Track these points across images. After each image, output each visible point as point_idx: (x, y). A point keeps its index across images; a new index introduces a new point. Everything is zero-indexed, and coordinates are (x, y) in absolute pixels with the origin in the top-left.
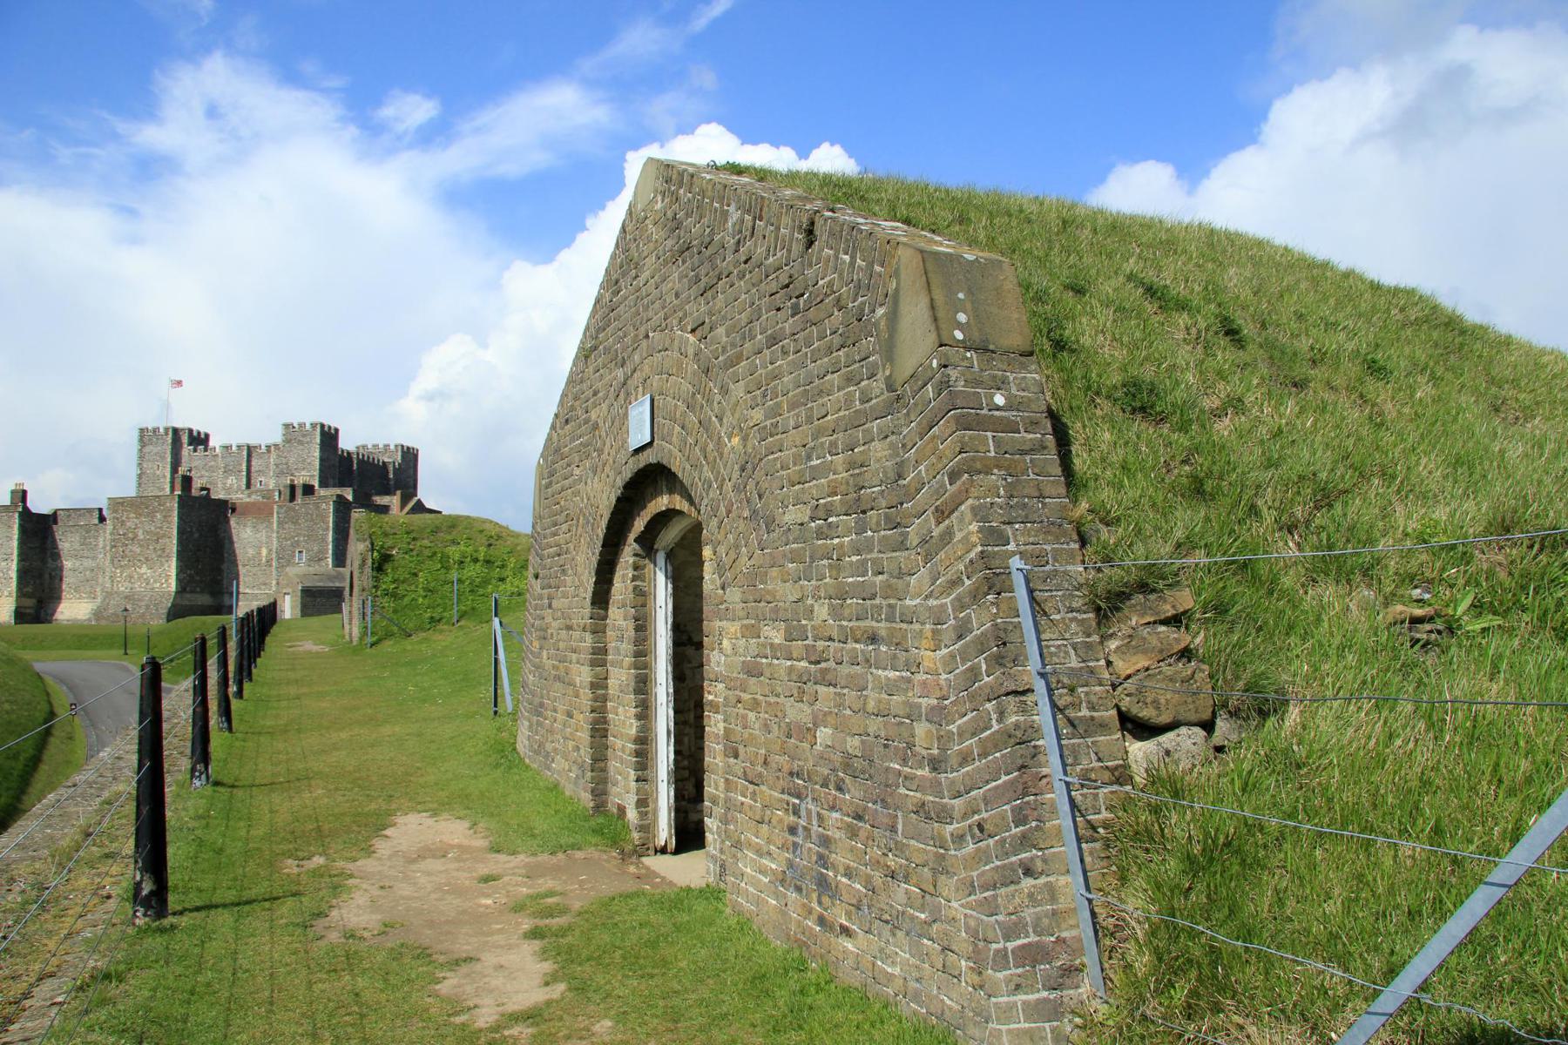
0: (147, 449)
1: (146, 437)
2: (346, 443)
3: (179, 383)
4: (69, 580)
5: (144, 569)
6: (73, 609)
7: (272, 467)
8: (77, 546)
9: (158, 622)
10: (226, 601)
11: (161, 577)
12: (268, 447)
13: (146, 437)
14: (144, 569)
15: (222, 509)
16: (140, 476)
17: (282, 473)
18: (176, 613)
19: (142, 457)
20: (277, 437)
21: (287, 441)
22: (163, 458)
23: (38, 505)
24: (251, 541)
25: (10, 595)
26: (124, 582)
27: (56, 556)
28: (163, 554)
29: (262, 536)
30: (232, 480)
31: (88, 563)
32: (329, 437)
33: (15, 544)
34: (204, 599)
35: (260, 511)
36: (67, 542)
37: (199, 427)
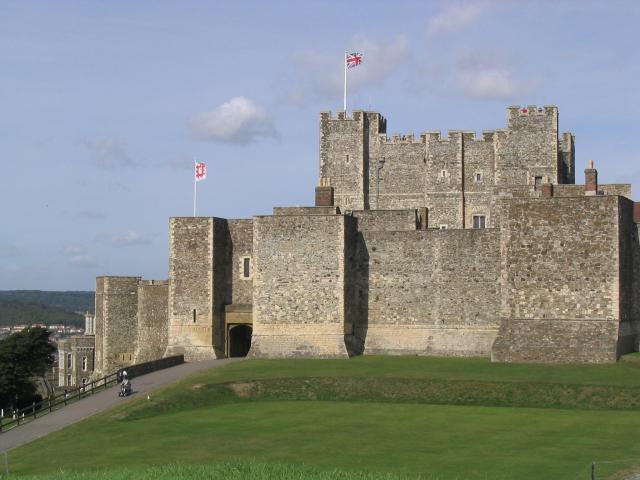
0: (332, 137)
3: (358, 60)
5: (565, 291)
7: (497, 158)
8: (400, 257)
12: (489, 137)
14: (565, 291)
16: (324, 169)
17: (509, 165)
19: (326, 146)
20: (501, 122)
21: (516, 128)
22: (353, 147)
25: (336, 319)
31: (421, 280)
33: (341, 255)
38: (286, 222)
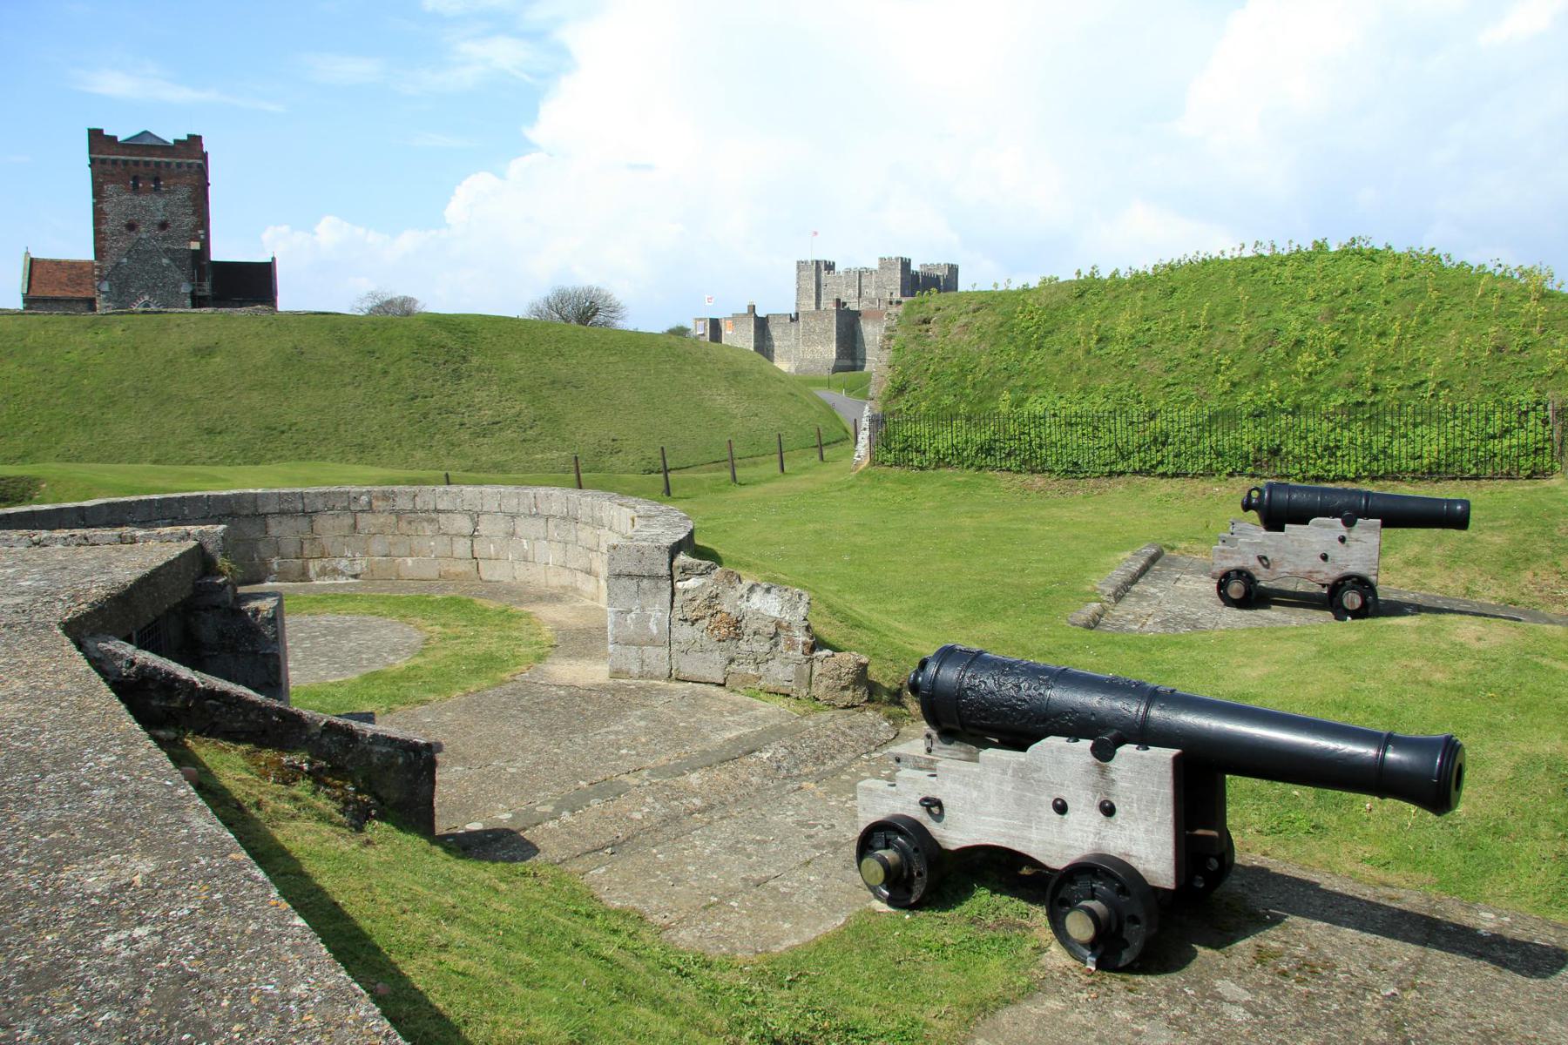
1: (801, 266)
2: (915, 267)
4: (777, 351)
6: (783, 365)
9: (826, 374)
10: (859, 363)
11: (830, 352)
13: (801, 266)
15: (857, 314)
18: (836, 369)
20: (875, 266)
23: (761, 313)
24: (871, 333)
26: (805, 353)
27: (770, 339)
28: (829, 340)
29: (877, 330)
30: (850, 291)
32: (906, 264)
34: (848, 363)
35: (876, 316)
36: (775, 332)
37: (829, 258)
38: (736, 318)
